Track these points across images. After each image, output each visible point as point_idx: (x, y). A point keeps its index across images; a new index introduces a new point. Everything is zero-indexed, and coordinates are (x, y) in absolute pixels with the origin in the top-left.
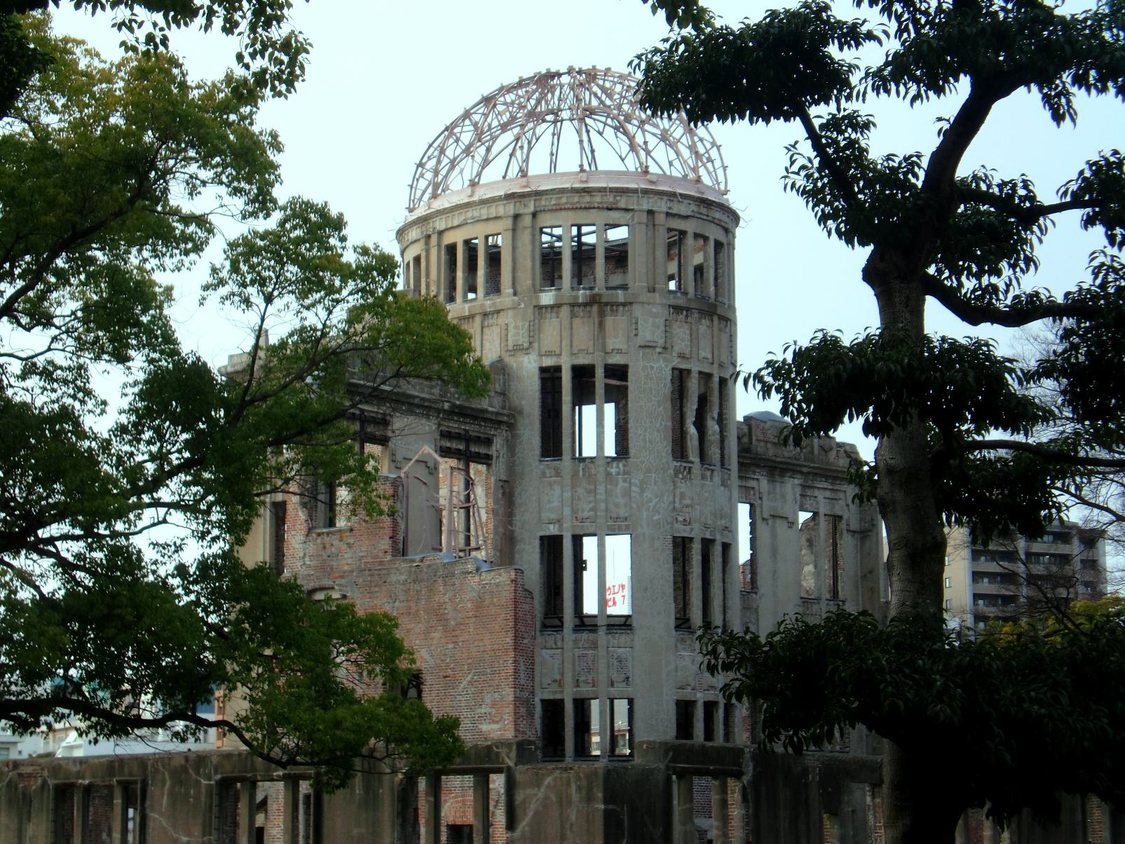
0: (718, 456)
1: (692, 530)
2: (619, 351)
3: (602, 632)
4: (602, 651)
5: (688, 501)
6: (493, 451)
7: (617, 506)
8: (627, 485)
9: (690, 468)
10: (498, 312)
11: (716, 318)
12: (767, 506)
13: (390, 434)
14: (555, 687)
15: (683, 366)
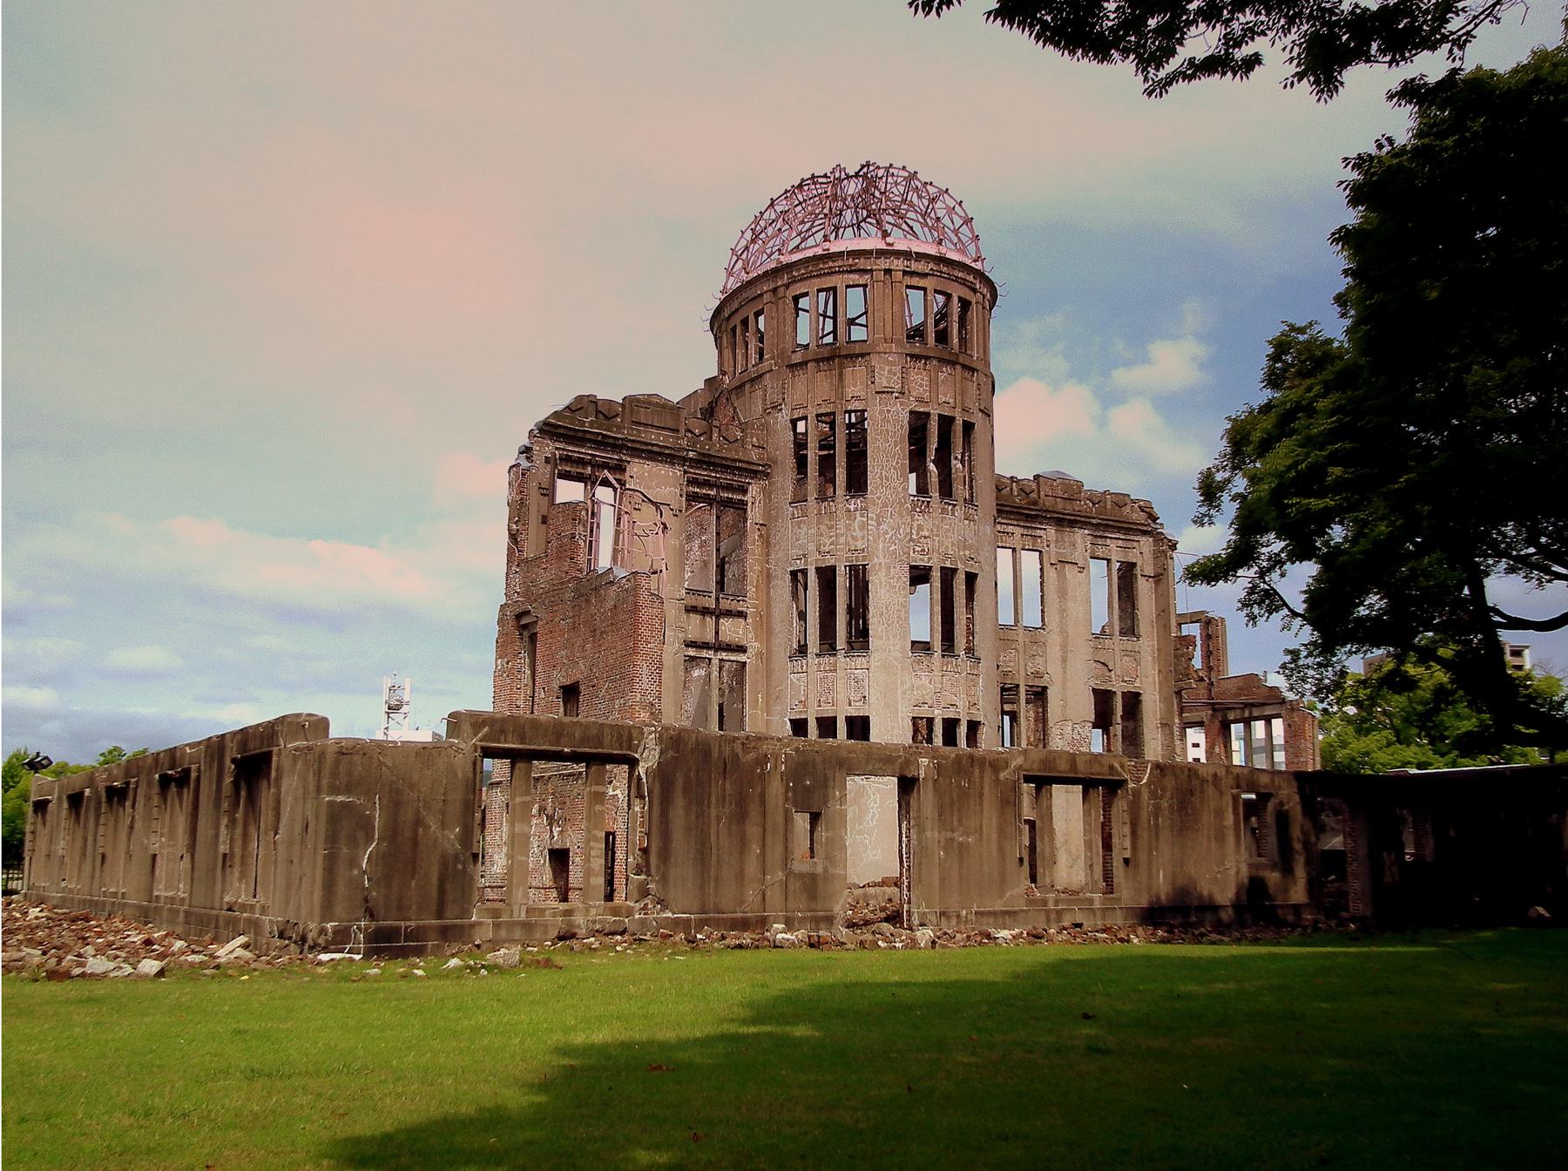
1: (930, 559)
2: (858, 398)
6: (748, 498)
7: (855, 539)
8: (865, 519)
9: (928, 502)
10: (761, 376)
11: (958, 367)
12: (1052, 553)
14: (800, 708)
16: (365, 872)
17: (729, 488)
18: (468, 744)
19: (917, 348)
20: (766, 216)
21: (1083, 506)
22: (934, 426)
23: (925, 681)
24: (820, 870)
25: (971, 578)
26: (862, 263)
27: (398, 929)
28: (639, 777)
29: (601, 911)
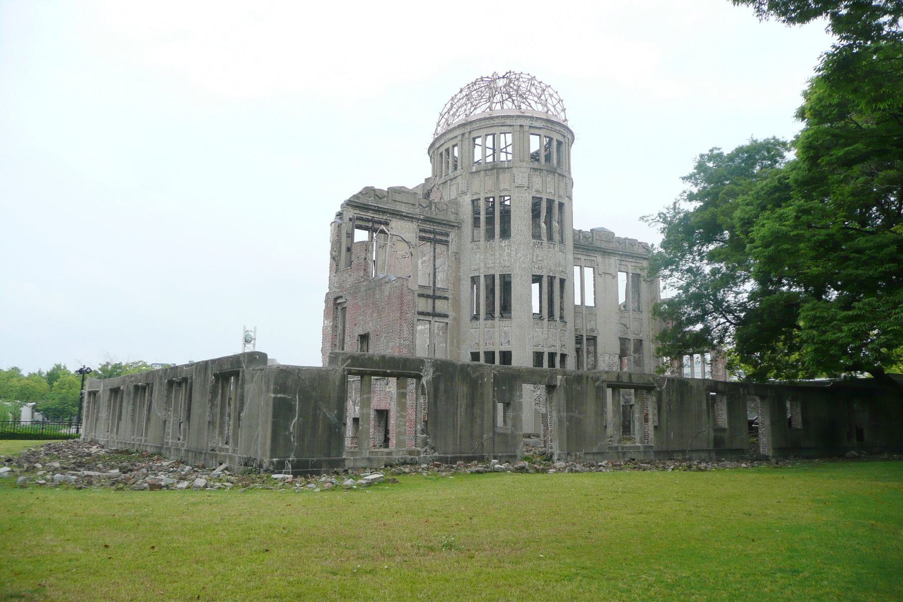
2: (506, 190)
4: (497, 329)
5: (540, 258)
6: (450, 239)
9: (541, 243)
10: (456, 178)
11: (556, 175)
12: (601, 268)
16: (291, 433)
17: (441, 234)
18: (340, 368)
19: (536, 165)
20: (458, 97)
22: (544, 205)
24: (509, 432)
25: (562, 281)
26: (508, 122)
27: (308, 461)
28: (423, 386)
29: (405, 453)
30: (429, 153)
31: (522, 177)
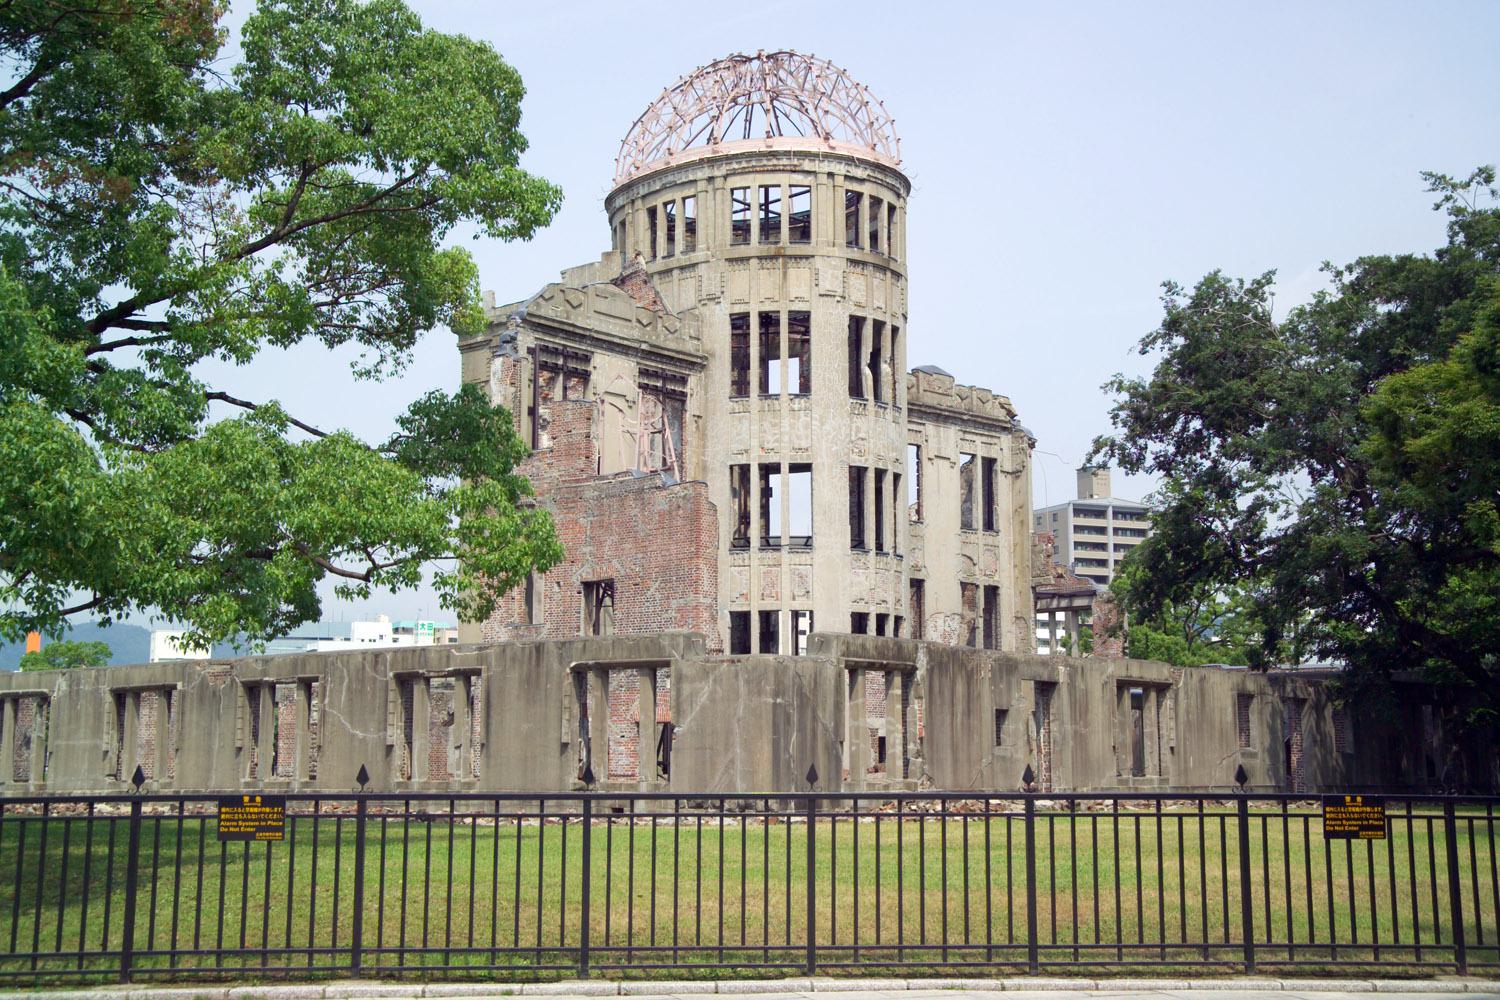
0: (890, 395)
1: (866, 460)
3: (785, 551)
4: (785, 568)
5: (861, 435)
7: (798, 437)
8: (809, 419)
10: (694, 265)
11: (889, 274)
13: (590, 369)
15: (859, 314)
17: (674, 379)
19: (855, 254)
21: (953, 402)
23: (862, 578)
26: (807, 165)
30: (609, 201)
31: (833, 275)
